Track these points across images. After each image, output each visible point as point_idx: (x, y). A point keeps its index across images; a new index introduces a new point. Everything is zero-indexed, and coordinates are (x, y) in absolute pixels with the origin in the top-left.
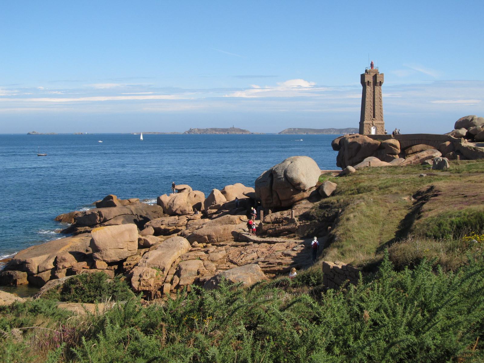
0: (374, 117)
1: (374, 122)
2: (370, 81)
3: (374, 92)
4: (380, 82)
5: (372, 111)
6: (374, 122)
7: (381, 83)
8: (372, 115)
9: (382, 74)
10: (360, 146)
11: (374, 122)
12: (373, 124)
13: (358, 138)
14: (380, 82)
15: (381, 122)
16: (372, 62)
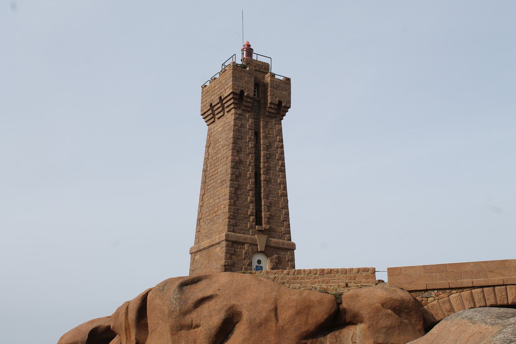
4: (280, 102)
7: (282, 108)
9: (288, 80)
14: (280, 102)
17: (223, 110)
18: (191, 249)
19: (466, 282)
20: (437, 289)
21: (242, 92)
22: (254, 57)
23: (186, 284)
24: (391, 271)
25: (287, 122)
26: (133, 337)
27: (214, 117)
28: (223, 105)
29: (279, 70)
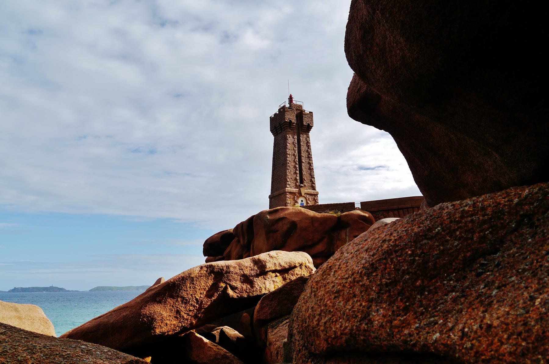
0: (302, 182)
1: (301, 189)
2: (293, 121)
3: (299, 141)
4: (309, 124)
5: (298, 172)
6: (303, 191)
7: (309, 128)
8: (298, 178)
10: (293, 225)
11: (303, 191)
12: (301, 193)
13: (287, 212)
14: (309, 124)
15: (312, 191)
16: (291, 96)
17: (281, 129)
18: (269, 196)
19: (395, 207)
20: (383, 211)
21: (290, 121)
22: (294, 102)
23: (270, 213)
24: (362, 204)
25: (311, 133)
26: (246, 238)
27: (277, 132)
28: (281, 127)
29: (307, 109)
